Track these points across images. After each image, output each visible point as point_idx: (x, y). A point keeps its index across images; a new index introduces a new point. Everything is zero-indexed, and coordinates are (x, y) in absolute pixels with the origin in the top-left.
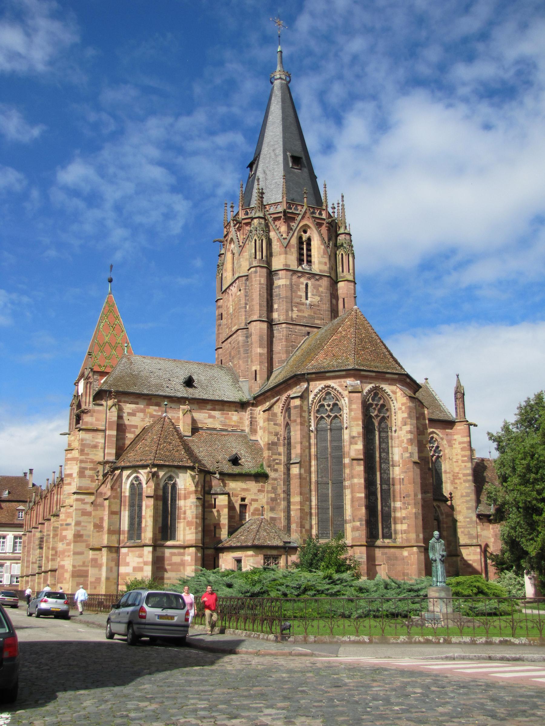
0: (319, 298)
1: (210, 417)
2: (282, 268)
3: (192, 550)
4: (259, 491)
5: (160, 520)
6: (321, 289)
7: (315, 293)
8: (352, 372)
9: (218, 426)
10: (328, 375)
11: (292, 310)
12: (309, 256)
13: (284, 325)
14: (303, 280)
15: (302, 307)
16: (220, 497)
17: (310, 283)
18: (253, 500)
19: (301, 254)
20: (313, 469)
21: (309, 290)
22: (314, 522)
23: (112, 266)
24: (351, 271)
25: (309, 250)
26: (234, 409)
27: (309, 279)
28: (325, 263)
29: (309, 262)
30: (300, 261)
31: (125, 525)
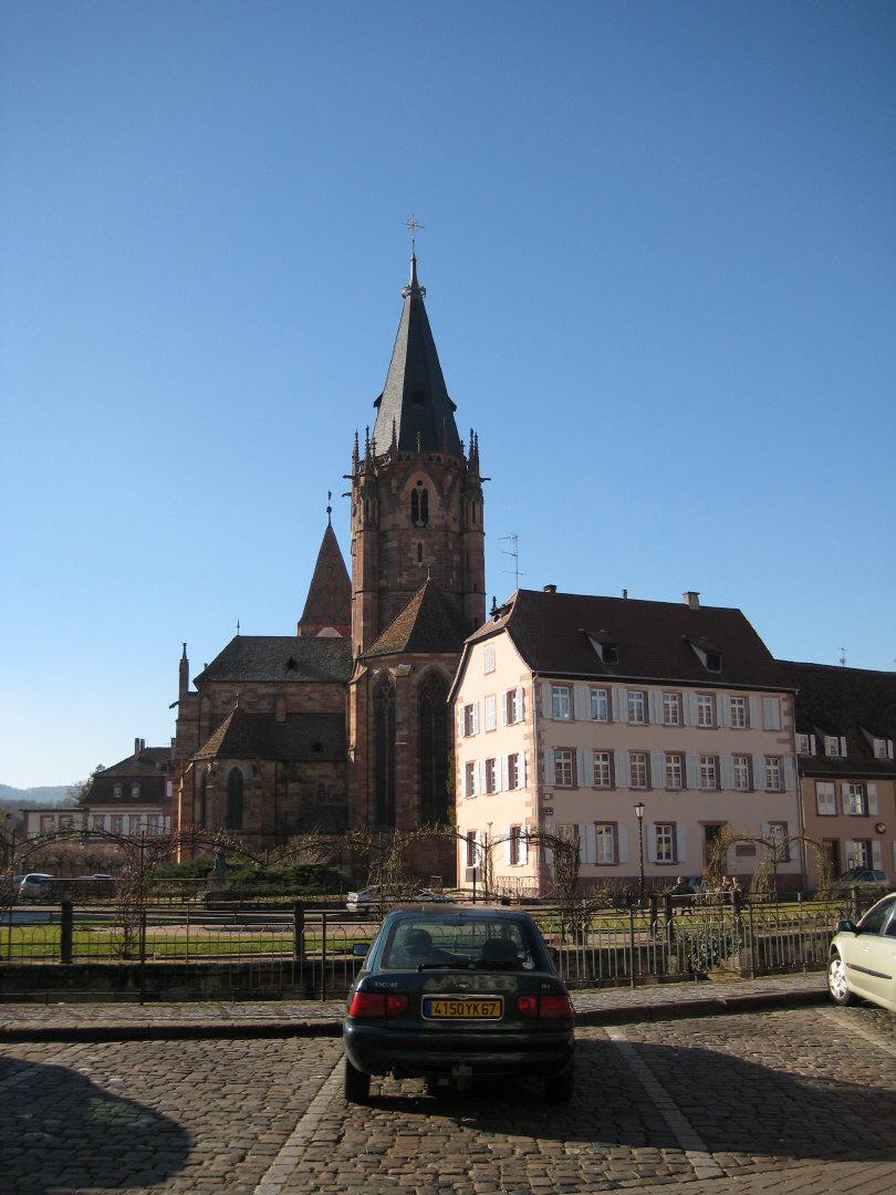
0: (434, 558)
1: (310, 699)
2: (390, 528)
3: (254, 837)
4: (338, 777)
5: (225, 809)
6: (436, 547)
7: (429, 552)
8: (402, 655)
9: (318, 709)
10: (383, 658)
11: (401, 575)
12: (425, 510)
13: (392, 594)
14: (416, 540)
15: (413, 570)
16: (291, 785)
17: (423, 542)
18: (332, 786)
19: (415, 510)
20: (371, 755)
21: (423, 550)
22: (371, 808)
23: (330, 494)
24: (477, 520)
25: (425, 503)
26: (335, 688)
27: (422, 536)
28: (443, 517)
29: (425, 517)
30: (414, 518)
31: (198, 817)
